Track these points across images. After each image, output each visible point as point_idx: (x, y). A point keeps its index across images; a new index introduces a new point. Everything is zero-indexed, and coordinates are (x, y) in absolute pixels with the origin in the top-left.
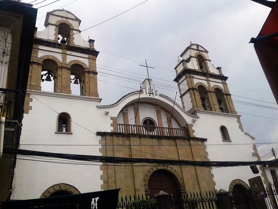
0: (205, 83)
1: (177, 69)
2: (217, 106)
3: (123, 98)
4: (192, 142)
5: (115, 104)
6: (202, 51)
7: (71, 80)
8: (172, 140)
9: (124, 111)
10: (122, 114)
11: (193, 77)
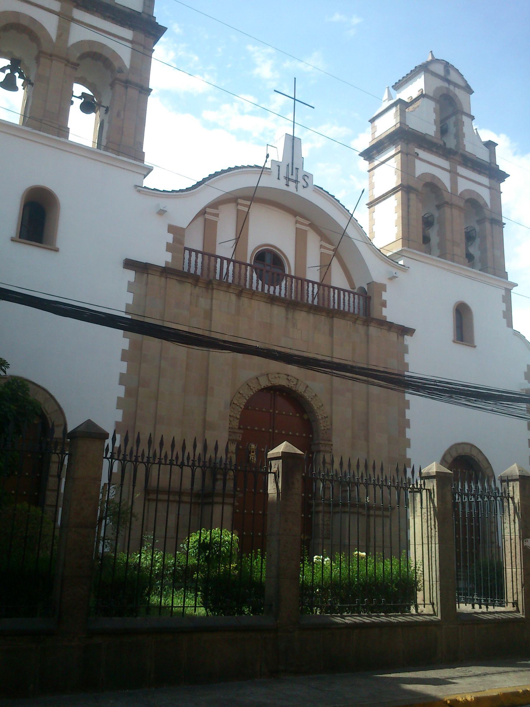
0: (445, 178)
1: (377, 122)
2: (460, 251)
3: (211, 176)
4: (373, 330)
5: (188, 189)
6: (456, 85)
7: (73, 99)
8: (323, 318)
9: (207, 216)
10: (200, 222)
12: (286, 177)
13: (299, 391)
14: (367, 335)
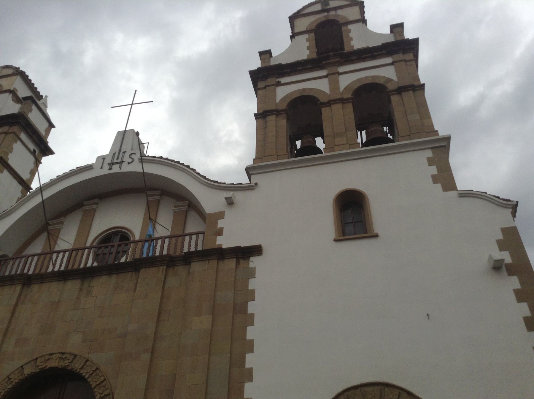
4: (197, 267)
6: (336, 9)
8: (129, 274)
9: (50, 228)
11: (279, 84)
12: (111, 163)
13: (74, 369)
14: (189, 273)
